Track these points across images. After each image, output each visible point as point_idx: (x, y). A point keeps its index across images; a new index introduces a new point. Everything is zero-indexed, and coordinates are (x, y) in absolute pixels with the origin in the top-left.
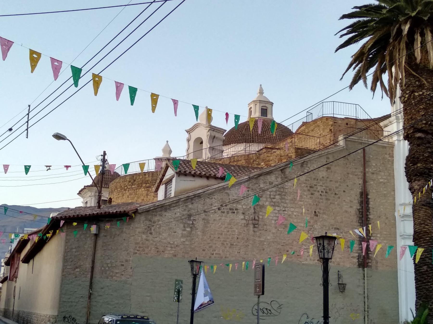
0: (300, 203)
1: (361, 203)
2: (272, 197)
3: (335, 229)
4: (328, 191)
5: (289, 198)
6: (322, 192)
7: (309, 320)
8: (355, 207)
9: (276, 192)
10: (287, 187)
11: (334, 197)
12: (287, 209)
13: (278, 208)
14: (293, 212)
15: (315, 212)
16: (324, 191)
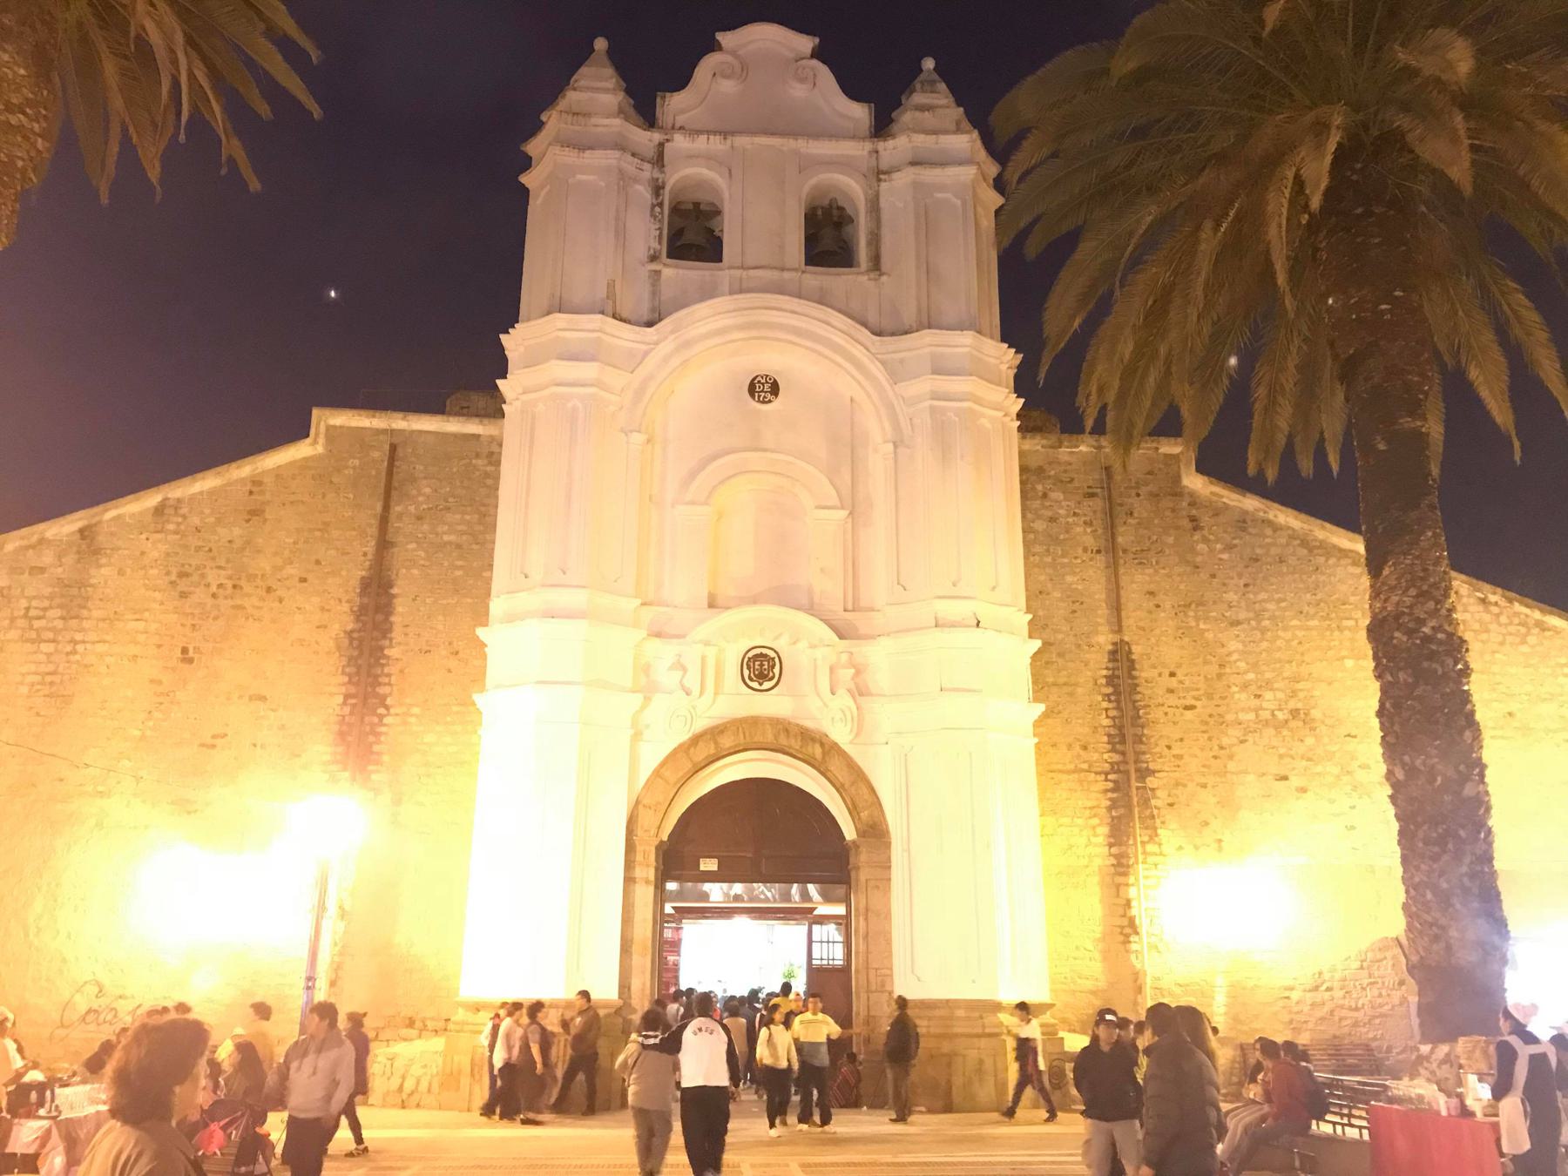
0: (133, 625)
1: (360, 613)
2: (32, 613)
3: (251, 699)
4: (243, 583)
5: (96, 614)
6: (220, 586)
7: (103, 1002)
8: (337, 626)
9: (51, 598)
10: (93, 581)
11: (262, 599)
12: (80, 648)
13: (45, 647)
14: (101, 656)
15: (185, 650)
16: (229, 584)
